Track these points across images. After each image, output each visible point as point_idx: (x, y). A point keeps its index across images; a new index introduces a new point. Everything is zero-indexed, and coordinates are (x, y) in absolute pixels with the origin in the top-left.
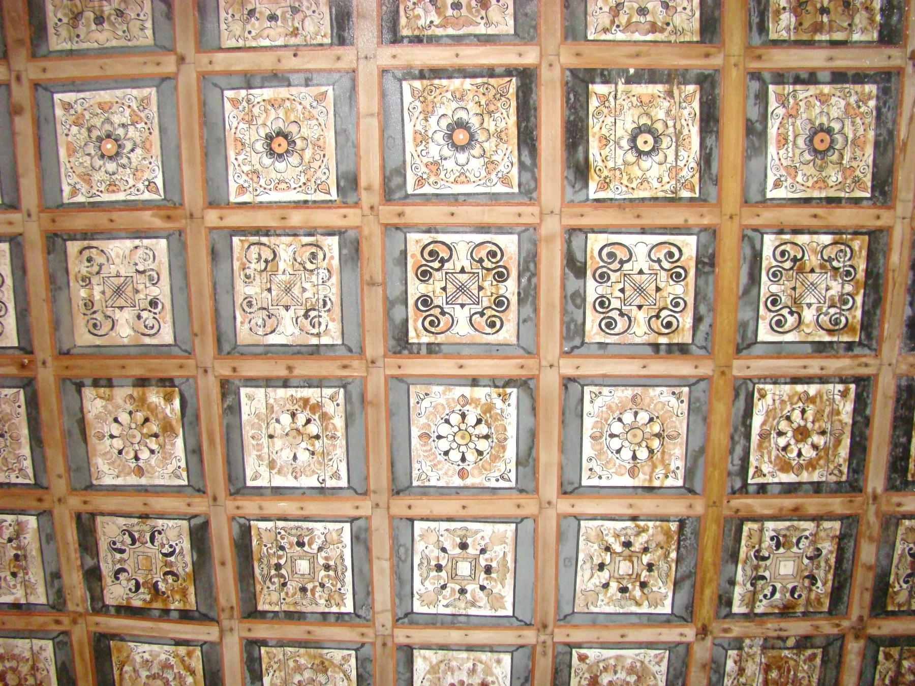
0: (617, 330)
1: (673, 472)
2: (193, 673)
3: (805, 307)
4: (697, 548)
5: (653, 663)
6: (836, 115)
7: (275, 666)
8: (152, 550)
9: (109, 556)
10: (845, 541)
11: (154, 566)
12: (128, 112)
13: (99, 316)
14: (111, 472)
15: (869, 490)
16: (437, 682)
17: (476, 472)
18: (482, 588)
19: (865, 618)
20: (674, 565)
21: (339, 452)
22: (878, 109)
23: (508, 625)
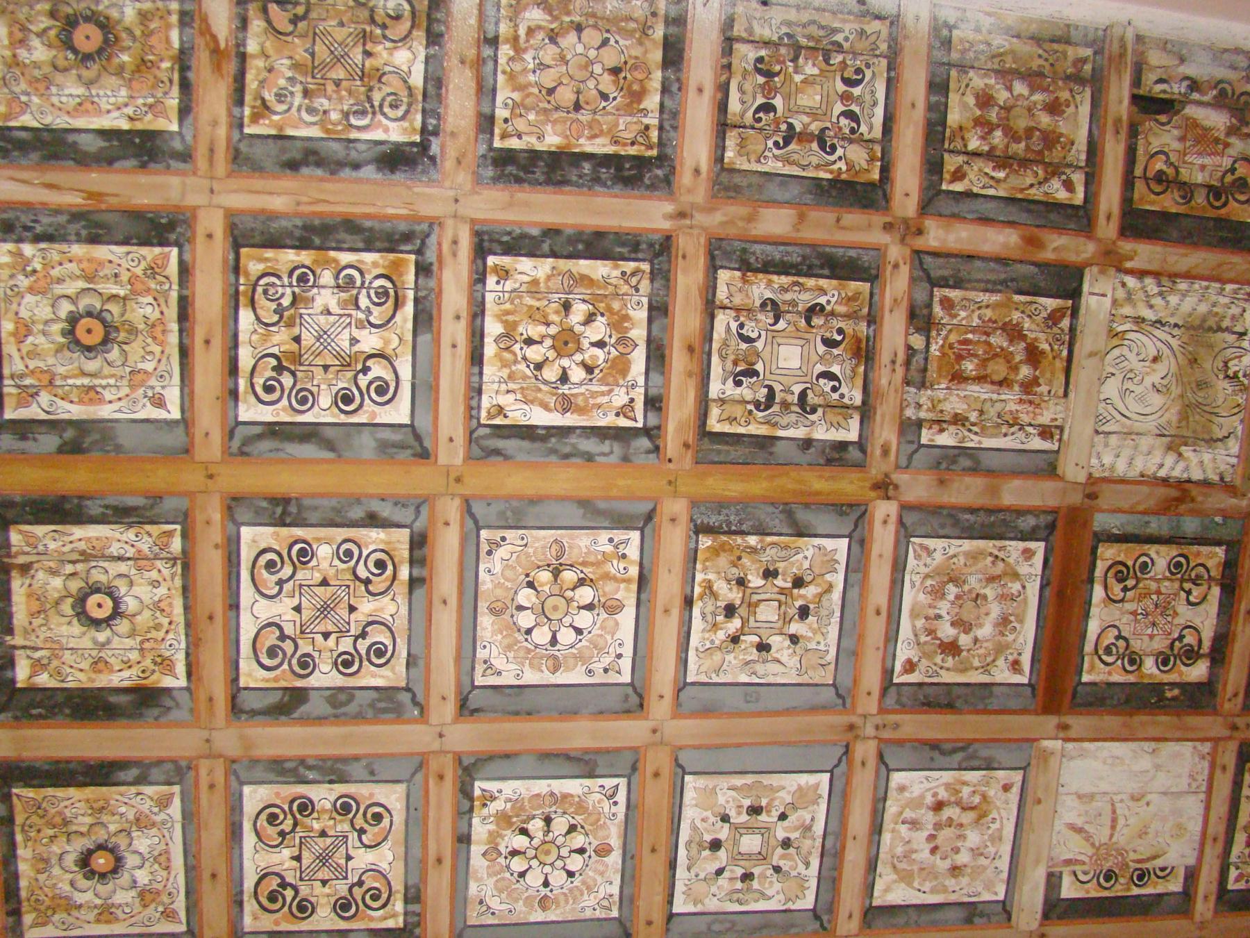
0: (388, 642)
1: (616, 547)
3: (356, 348)
4: (744, 503)
5: (929, 561)
6: (49, 309)
10: (752, 260)
15: (666, 225)
16: (925, 873)
17: (601, 833)
18: (783, 817)
19: (888, 219)
20: (769, 539)
22: (37, 239)
23: (843, 780)
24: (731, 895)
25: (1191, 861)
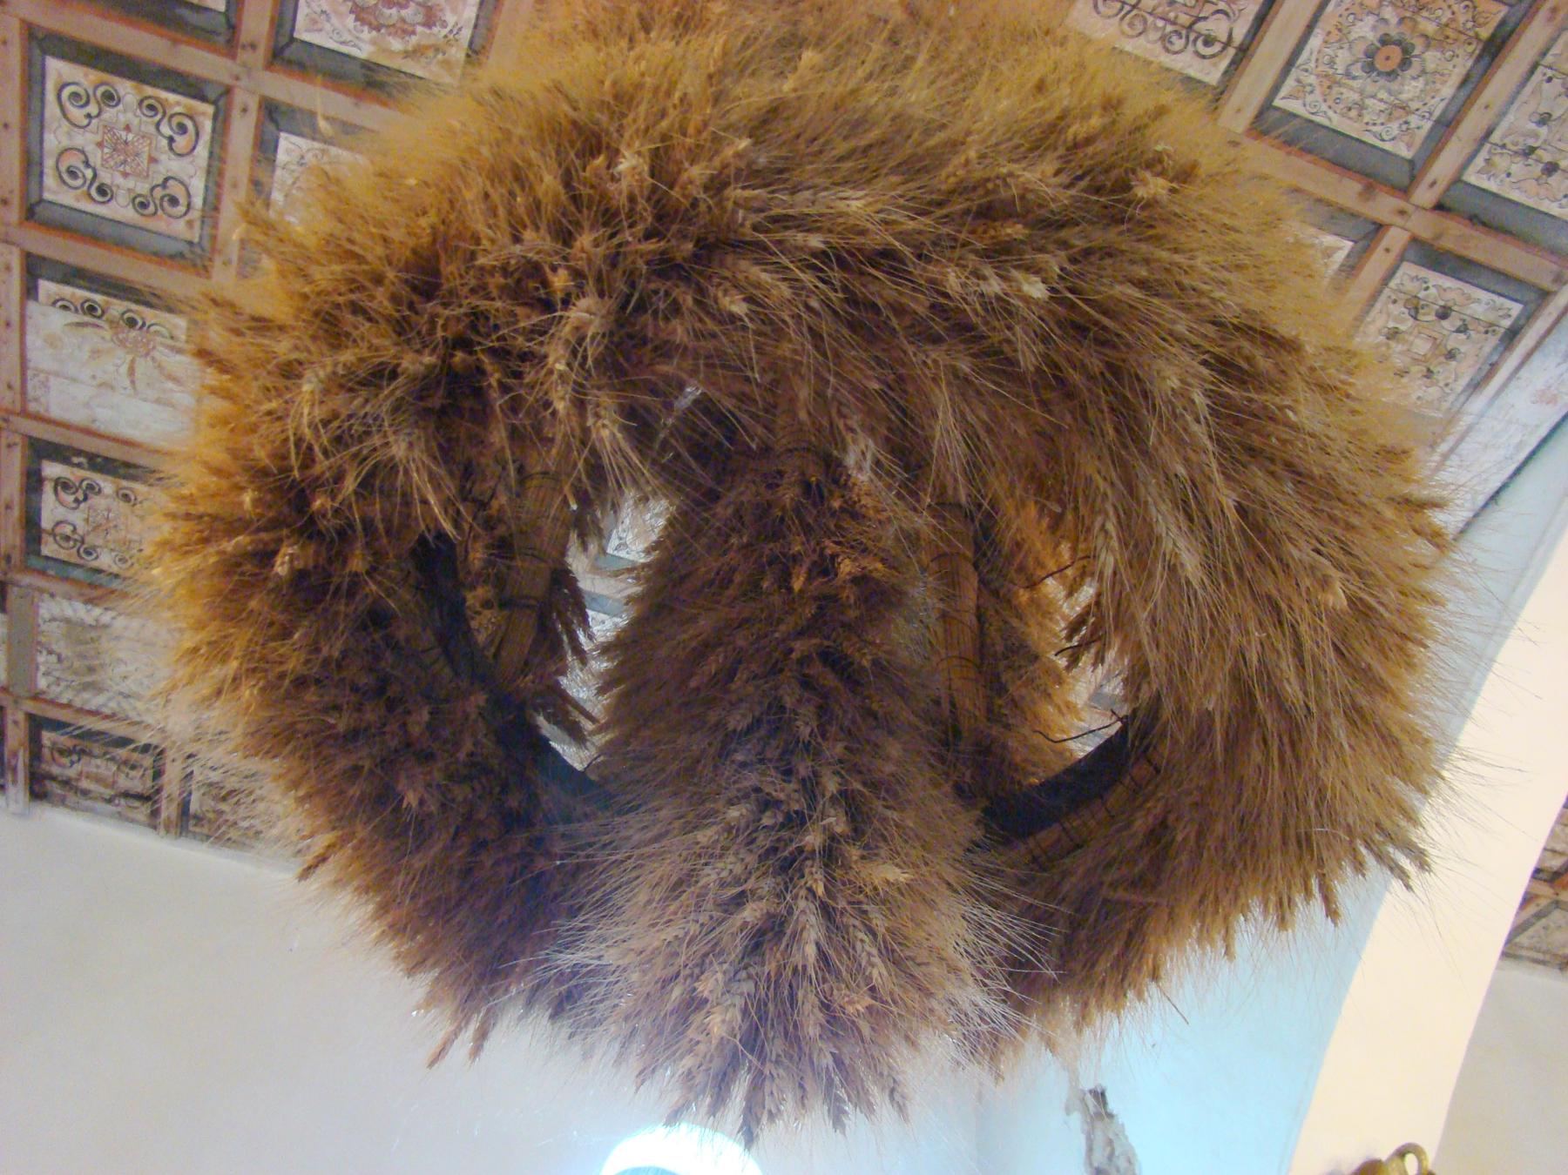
2: (407, 54)
25: (32, 306)
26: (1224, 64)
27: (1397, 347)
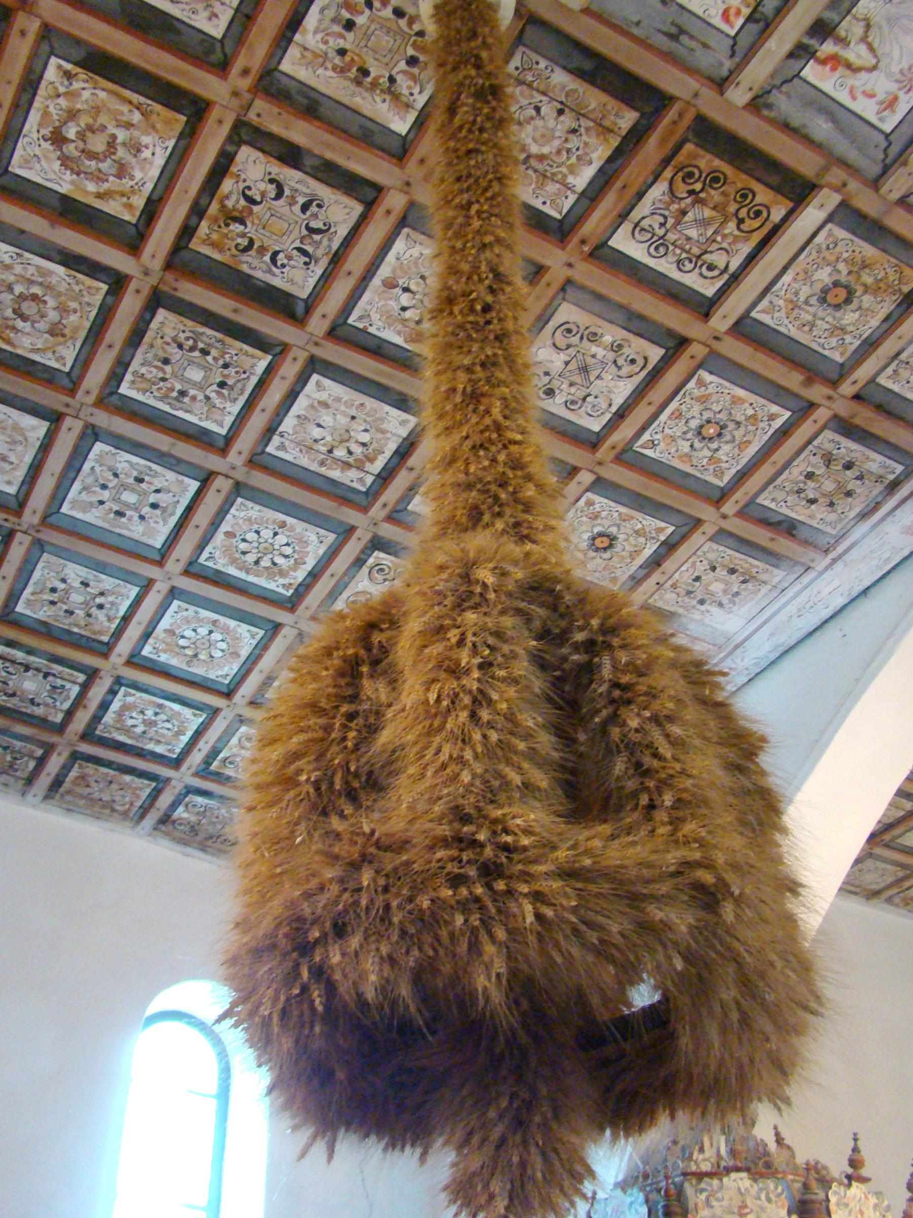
2: (99, 196)
7: (76, 288)
8: (290, 243)
9: (308, 191)
11: (268, 234)
12: (724, 458)
13: (575, 340)
14: (407, 255)
17: (227, 543)
21: (304, 461)
24: (156, 474)
26: (719, 284)
27: (811, 484)
